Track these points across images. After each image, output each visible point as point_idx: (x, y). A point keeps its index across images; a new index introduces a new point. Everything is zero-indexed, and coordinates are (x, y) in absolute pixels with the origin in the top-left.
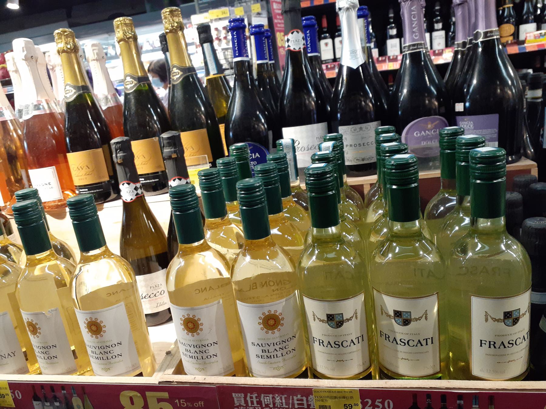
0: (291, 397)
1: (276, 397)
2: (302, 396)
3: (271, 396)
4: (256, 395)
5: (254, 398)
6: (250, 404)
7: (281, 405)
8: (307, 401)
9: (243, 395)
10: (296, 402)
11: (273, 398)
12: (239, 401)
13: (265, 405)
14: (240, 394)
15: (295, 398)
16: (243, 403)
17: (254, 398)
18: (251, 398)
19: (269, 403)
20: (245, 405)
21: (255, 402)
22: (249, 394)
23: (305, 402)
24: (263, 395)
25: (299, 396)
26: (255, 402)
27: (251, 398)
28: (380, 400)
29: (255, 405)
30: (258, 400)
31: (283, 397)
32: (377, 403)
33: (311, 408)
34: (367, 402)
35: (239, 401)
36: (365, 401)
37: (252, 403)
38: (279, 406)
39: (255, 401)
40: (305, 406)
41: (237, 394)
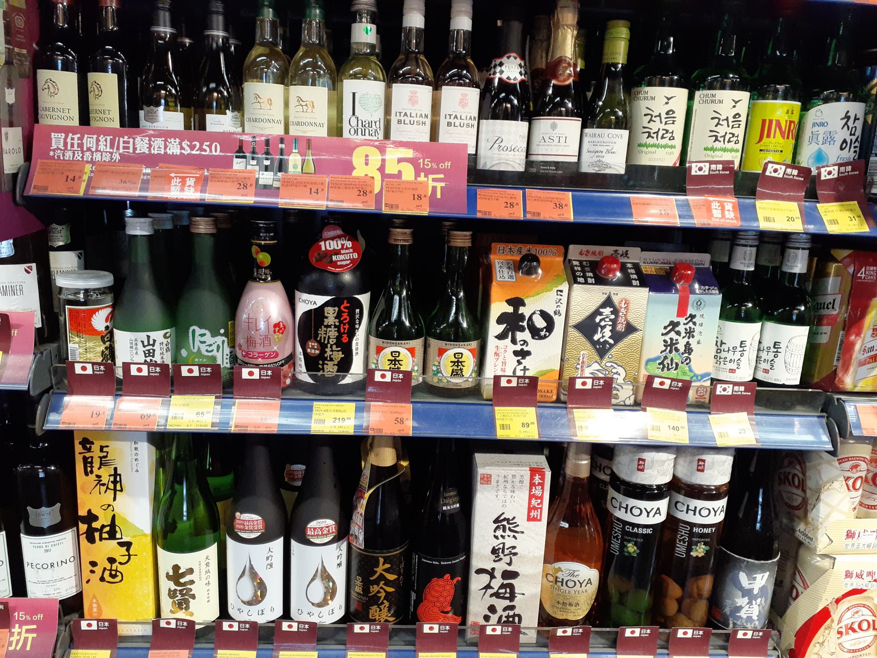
1: (100, 138)
2: (129, 138)
3: (95, 137)
4: (79, 135)
5: (76, 139)
6: (69, 148)
8: (134, 143)
9: (63, 135)
10: (121, 145)
11: (98, 141)
12: (58, 143)
13: (87, 148)
14: (59, 134)
15: (121, 140)
16: (61, 146)
17: (76, 139)
18: (73, 139)
19: (91, 146)
21: (76, 146)
22: (70, 135)
23: (131, 145)
24: (86, 136)
25: (126, 138)
26: (76, 146)
27: (73, 139)
28: (208, 143)
29: (76, 148)
30: (80, 142)
31: (109, 138)
32: (204, 147)
33: (137, 152)
34: (195, 146)
35: (58, 143)
37: (72, 145)
39: (76, 142)
40: (131, 151)
41: (56, 134)
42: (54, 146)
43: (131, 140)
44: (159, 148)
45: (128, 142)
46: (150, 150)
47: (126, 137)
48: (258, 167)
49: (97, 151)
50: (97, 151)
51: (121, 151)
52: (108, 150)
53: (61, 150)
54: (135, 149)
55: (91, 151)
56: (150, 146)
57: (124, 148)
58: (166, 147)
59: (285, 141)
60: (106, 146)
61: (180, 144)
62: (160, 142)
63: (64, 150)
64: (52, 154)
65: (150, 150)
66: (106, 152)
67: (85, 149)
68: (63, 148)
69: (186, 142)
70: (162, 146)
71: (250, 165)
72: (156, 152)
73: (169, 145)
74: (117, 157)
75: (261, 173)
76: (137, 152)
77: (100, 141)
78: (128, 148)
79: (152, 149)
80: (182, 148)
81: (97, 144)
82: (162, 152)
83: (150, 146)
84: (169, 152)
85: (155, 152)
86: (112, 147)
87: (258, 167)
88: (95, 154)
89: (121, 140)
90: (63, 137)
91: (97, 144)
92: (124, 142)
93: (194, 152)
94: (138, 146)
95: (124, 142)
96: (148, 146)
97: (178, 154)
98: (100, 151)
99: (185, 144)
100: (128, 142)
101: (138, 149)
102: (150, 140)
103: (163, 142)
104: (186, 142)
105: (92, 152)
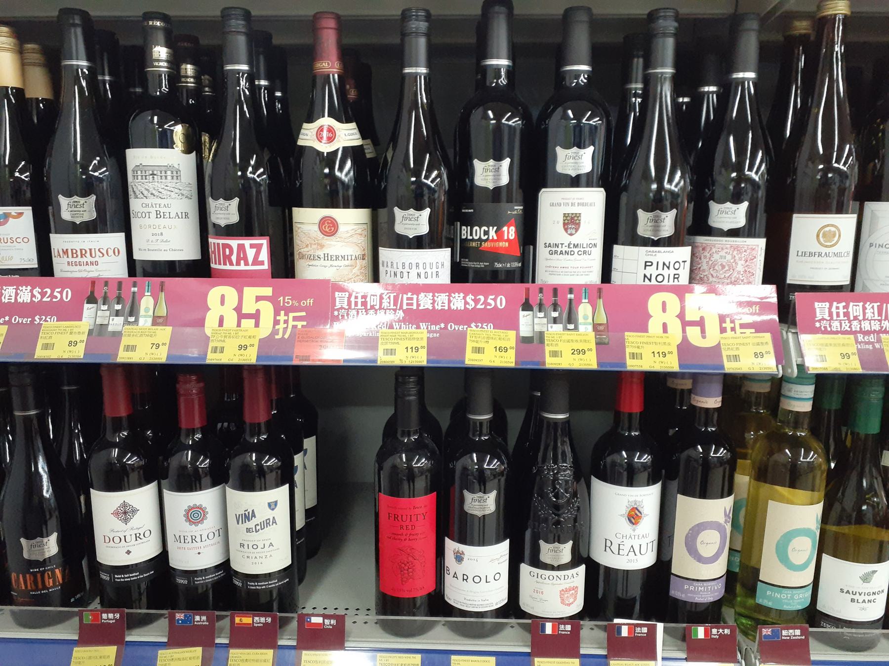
0: (401, 295)
6: (353, 306)
7: (388, 305)
8: (418, 301)
10: (405, 302)
12: (341, 302)
16: (345, 306)
19: (375, 304)
20: (347, 307)
23: (415, 302)
25: (409, 295)
28: (493, 297)
32: (489, 301)
34: (480, 299)
36: (478, 298)
38: (385, 308)
40: (415, 307)
42: (338, 305)
43: (415, 297)
44: (443, 303)
45: (412, 299)
46: (434, 307)
47: (410, 294)
48: (546, 319)
49: (380, 308)
50: (380, 308)
51: (405, 307)
52: (392, 307)
53: (345, 309)
54: (418, 305)
55: (375, 309)
56: (434, 301)
57: (408, 304)
58: (449, 301)
59: (574, 290)
60: (389, 303)
61: (464, 298)
62: (444, 297)
63: (348, 309)
64: (336, 313)
65: (434, 307)
66: (390, 309)
67: (369, 307)
68: (347, 307)
69: (470, 296)
70: (446, 302)
71: (537, 317)
72: (440, 308)
73: (454, 300)
74: (401, 314)
75: (549, 325)
76: (420, 308)
77: (383, 299)
78: (412, 304)
79: (436, 305)
80: (466, 303)
81: (381, 303)
82: (446, 308)
83: (434, 301)
84: (453, 307)
85: (438, 307)
86: (395, 304)
87: (546, 319)
88: (378, 312)
89: (405, 296)
90: (347, 296)
91: (381, 303)
92: (408, 299)
93: (479, 306)
94: (421, 303)
95: (408, 299)
96: (432, 301)
97: (463, 308)
98: (383, 309)
99: (470, 298)
100: (412, 299)
101: (422, 305)
102: (433, 296)
103: (447, 297)
104: (470, 296)
105: (376, 310)
